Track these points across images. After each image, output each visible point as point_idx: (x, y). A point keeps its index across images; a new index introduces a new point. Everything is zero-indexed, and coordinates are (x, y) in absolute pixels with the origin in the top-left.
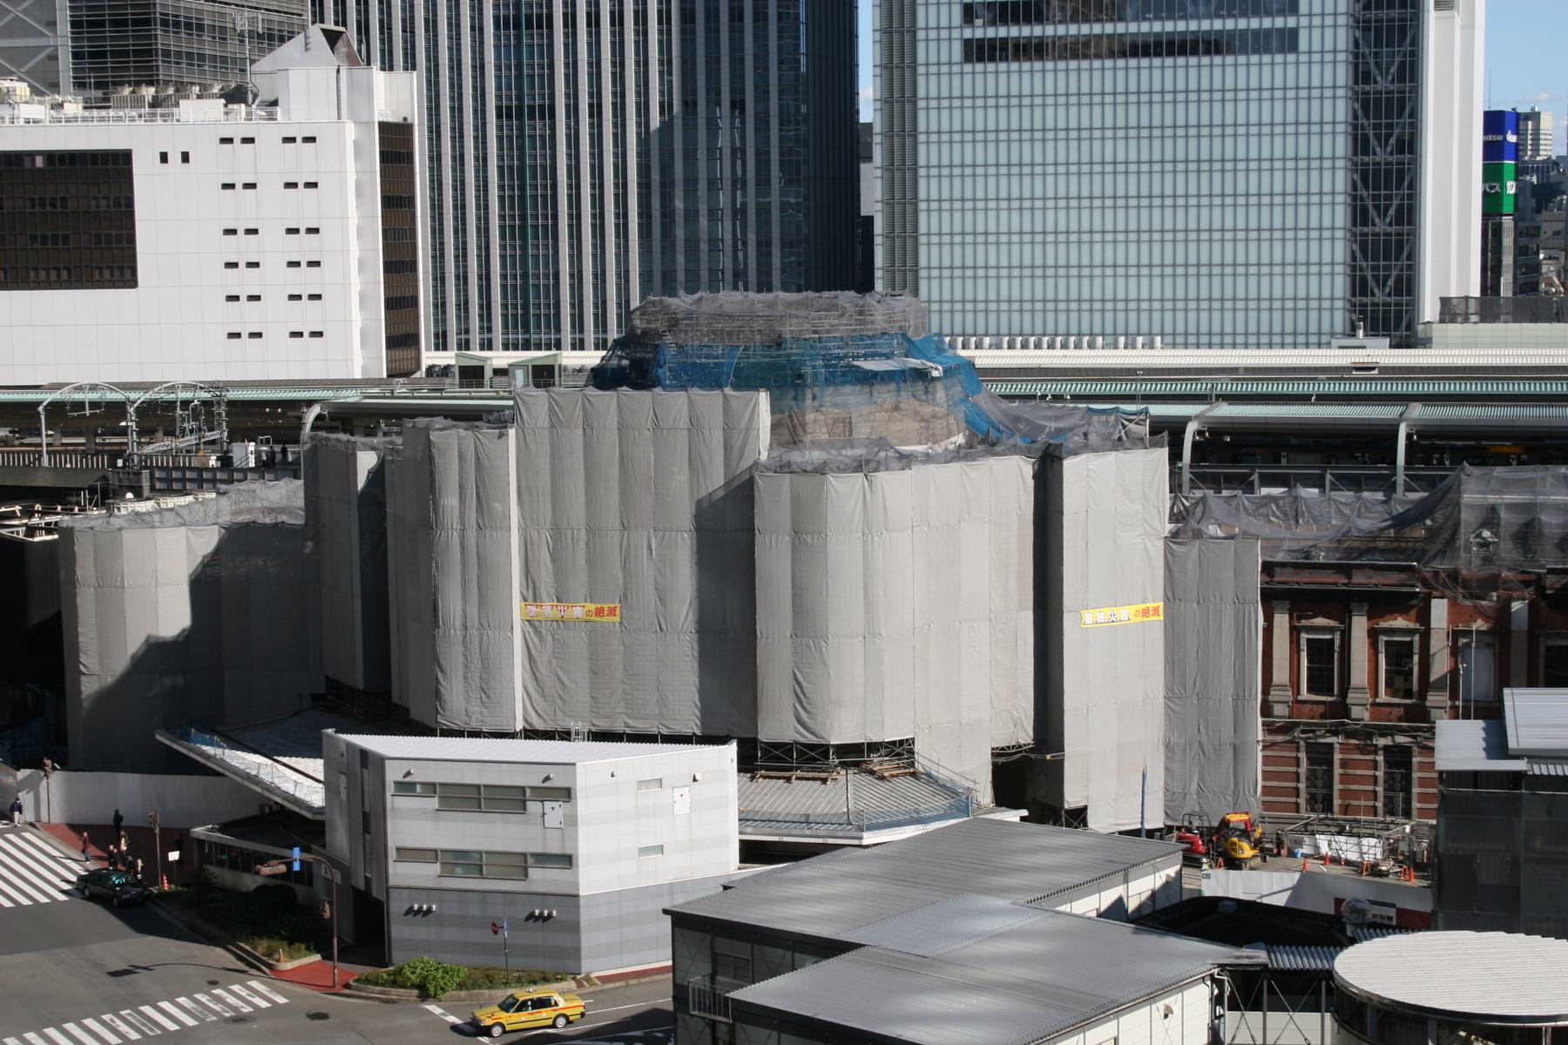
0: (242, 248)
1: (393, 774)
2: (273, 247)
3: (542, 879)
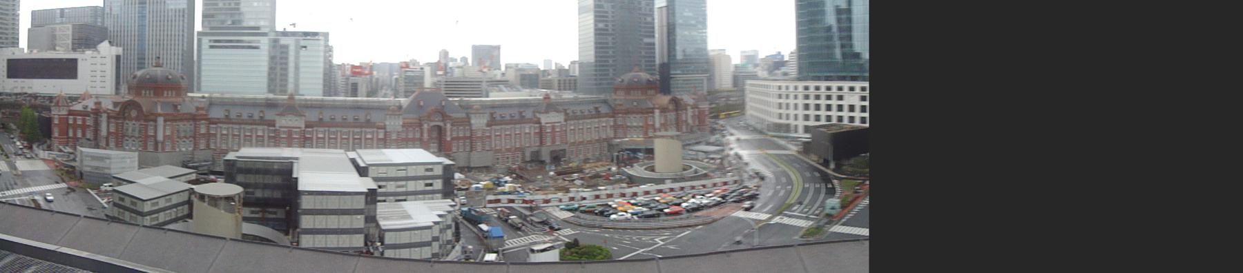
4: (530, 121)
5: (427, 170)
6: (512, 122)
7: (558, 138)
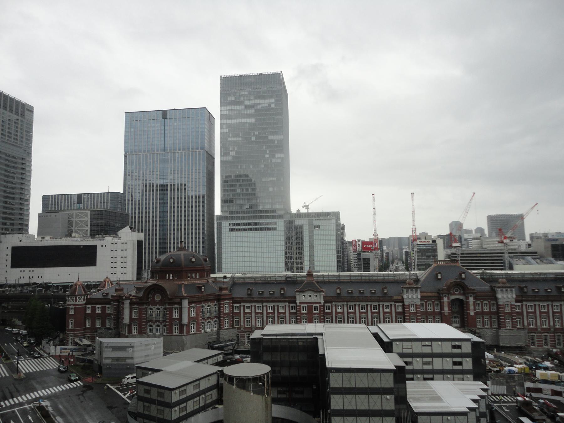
0: (114, 260)
1: (105, 345)
2: (119, 259)
3: (129, 361)
5: (454, 347)
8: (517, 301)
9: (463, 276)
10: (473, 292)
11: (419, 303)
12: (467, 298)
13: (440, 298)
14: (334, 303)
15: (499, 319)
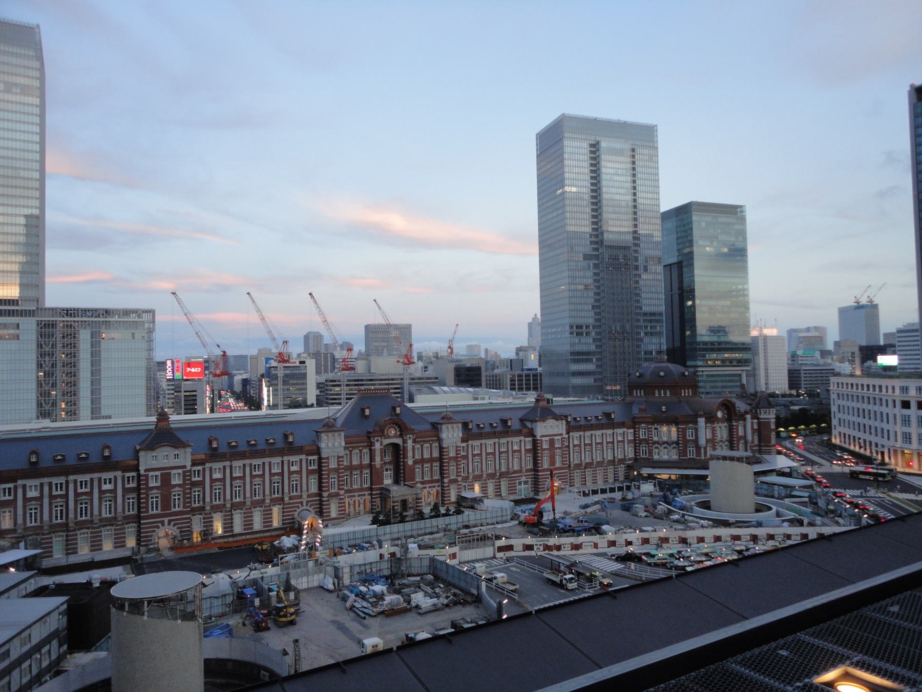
4: (518, 433)
6: (494, 434)
7: (558, 459)
8: (463, 441)
9: (398, 410)
10: (412, 431)
11: (342, 454)
12: (405, 442)
13: (371, 445)
14: (208, 465)
15: (441, 466)
